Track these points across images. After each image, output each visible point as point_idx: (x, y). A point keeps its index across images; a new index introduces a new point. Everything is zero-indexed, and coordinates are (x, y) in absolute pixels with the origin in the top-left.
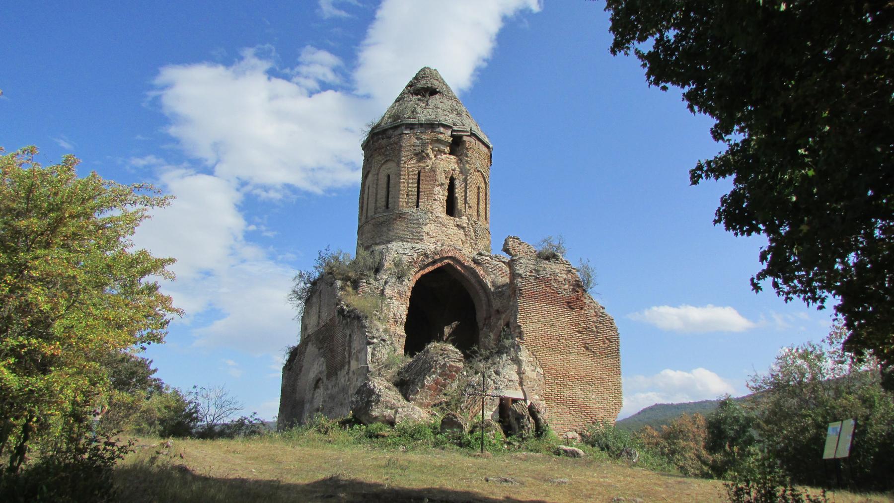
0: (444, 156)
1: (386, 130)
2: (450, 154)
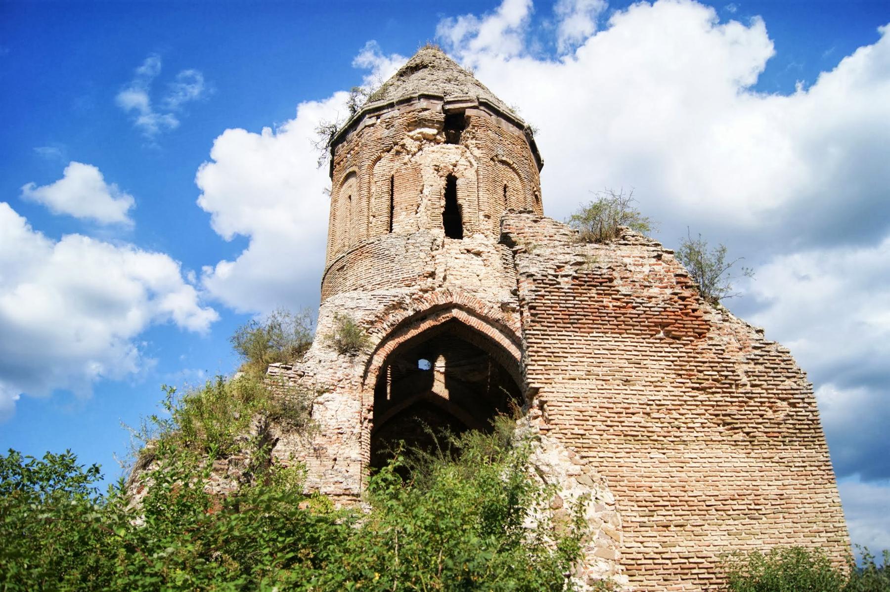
0: (436, 147)
2: (446, 142)
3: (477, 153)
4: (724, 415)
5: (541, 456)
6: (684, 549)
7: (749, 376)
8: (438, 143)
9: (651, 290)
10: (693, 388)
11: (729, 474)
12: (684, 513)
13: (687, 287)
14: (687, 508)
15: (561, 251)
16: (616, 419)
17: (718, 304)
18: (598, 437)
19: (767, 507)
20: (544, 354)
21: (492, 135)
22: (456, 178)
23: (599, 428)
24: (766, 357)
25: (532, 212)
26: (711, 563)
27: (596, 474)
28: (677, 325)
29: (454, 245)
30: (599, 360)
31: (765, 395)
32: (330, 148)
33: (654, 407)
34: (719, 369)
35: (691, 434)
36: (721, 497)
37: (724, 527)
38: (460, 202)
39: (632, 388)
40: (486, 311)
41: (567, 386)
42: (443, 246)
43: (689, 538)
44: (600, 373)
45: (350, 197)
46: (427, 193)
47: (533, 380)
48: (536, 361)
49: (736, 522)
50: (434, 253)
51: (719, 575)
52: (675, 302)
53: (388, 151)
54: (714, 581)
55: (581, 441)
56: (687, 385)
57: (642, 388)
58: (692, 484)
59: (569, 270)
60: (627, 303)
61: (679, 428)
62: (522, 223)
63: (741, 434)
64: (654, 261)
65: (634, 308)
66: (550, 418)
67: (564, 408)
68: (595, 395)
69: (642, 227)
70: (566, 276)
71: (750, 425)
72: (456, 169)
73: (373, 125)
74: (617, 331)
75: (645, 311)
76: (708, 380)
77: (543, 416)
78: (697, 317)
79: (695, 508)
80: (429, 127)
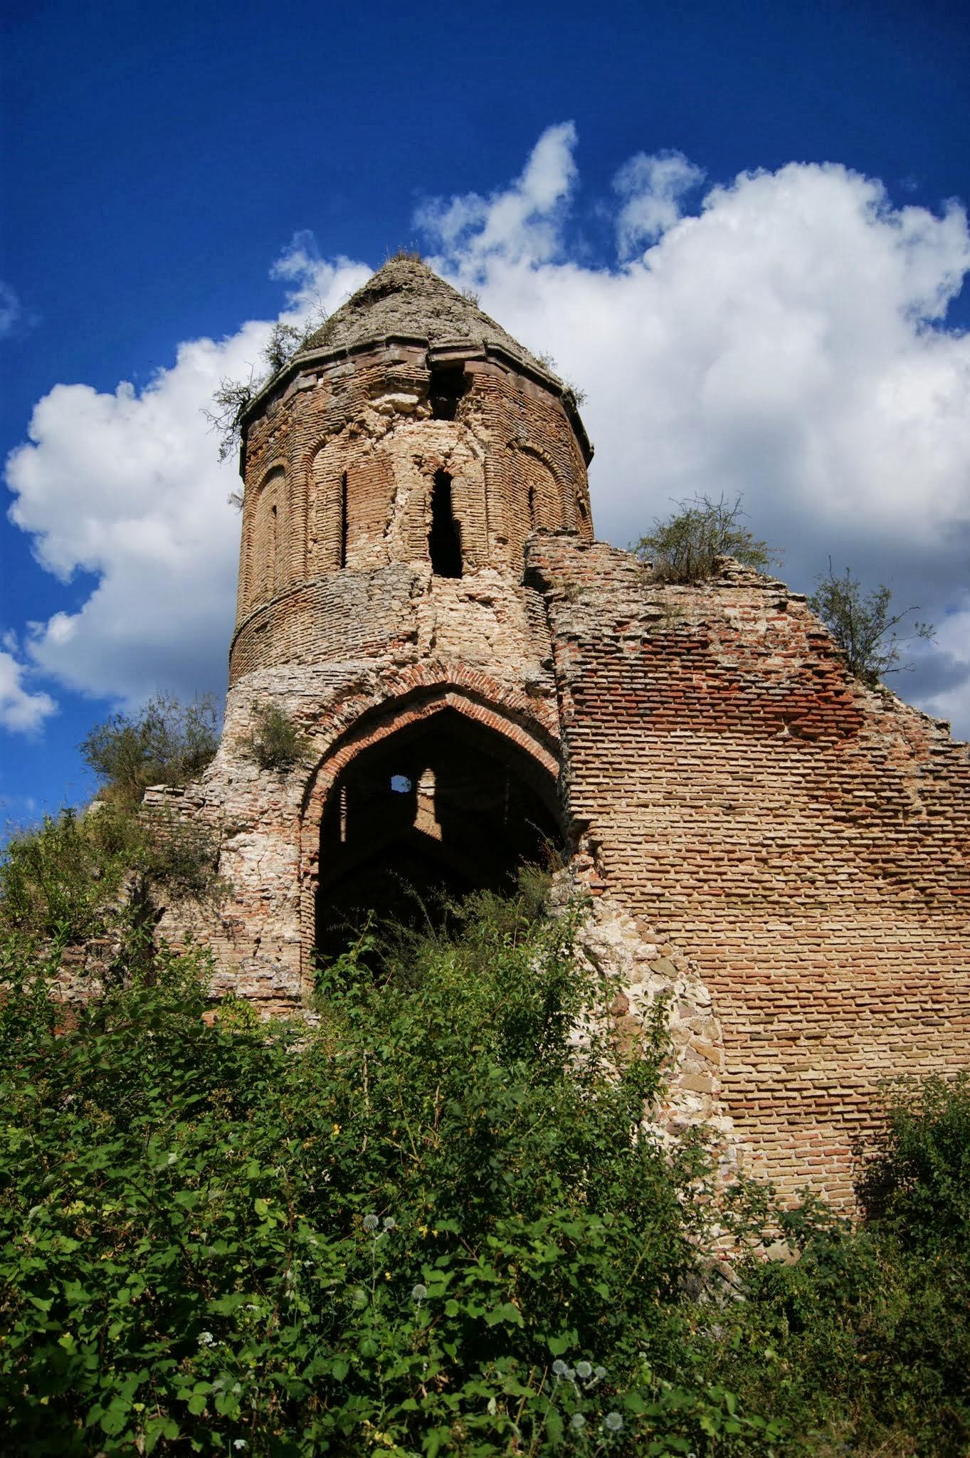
0: (416, 426)
3: (485, 434)
4: (885, 861)
5: (593, 930)
6: (822, 1075)
7: (925, 799)
8: (420, 419)
9: (769, 661)
10: (837, 819)
11: (892, 955)
12: (821, 1017)
13: (828, 655)
14: (825, 1009)
15: (624, 598)
16: (713, 869)
17: (876, 682)
18: (684, 898)
19: (952, 1005)
20: (597, 765)
21: (509, 405)
22: (450, 477)
23: (685, 883)
24: (951, 768)
25: (576, 533)
26: (863, 1095)
27: (681, 957)
28: (810, 717)
29: (449, 589)
30: (685, 775)
31: (950, 828)
32: (239, 427)
33: (774, 849)
34: (878, 787)
35: (833, 892)
36: (879, 992)
37: (884, 1039)
38: (457, 516)
39: (738, 819)
40: (501, 696)
41: (634, 816)
42: (430, 590)
43: (829, 1057)
44: (688, 796)
45: (274, 509)
46: (402, 503)
47: (580, 808)
48: (583, 777)
49: (903, 1031)
50: (415, 601)
51: (876, 1115)
52: (808, 680)
53: (337, 432)
54: (869, 1123)
55: (657, 904)
56: (828, 813)
57: (755, 819)
58: (833, 971)
59: (636, 628)
60: (731, 681)
61: (813, 882)
62: (560, 552)
63: (912, 890)
64: (773, 613)
65: (742, 689)
66: (607, 868)
67: (630, 853)
68: (680, 831)
69: (755, 558)
70: (632, 638)
71: (926, 877)
72: (449, 462)
73: (311, 388)
74: (714, 727)
75: (759, 695)
76: (859, 804)
77: (595, 865)
78: (843, 704)
79: (839, 1009)
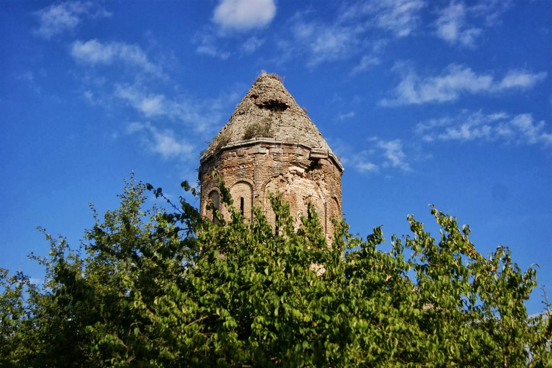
1: (238, 147)
3: (326, 192)
53: (275, 177)
80: (301, 167)
